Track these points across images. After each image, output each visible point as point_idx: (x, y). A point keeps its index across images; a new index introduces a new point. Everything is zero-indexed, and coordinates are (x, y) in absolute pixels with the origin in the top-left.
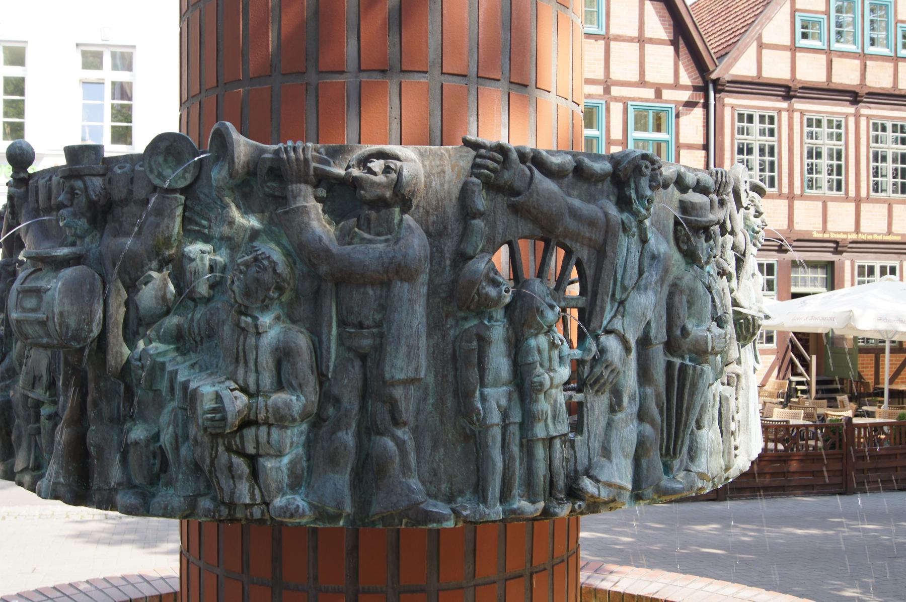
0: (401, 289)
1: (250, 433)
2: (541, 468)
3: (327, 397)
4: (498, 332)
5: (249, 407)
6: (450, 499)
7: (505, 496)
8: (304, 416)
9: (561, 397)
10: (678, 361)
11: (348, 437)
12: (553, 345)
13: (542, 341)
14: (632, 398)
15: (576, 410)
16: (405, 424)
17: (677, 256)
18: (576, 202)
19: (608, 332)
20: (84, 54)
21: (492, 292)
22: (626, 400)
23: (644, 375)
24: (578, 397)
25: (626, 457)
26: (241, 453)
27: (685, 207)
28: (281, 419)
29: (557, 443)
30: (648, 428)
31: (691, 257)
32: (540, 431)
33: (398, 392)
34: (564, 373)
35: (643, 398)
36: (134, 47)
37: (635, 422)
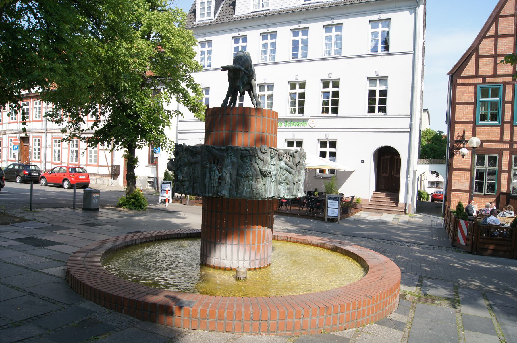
0: (197, 165)
1: (183, 182)
2: (213, 191)
3: (191, 179)
4: (208, 171)
5: (183, 179)
6: (202, 193)
7: (208, 194)
8: (188, 181)
9: (217, 181)
10: (238, 177)
11: (192, 184)
12: (215, 173)
13: (213, 173)
14: (228, 182)
15: (219, 183)
16: (198, 183)
17: (240, 161)
18: (220, 153)
19: (224, 172)
20: (324, 83)
21: (206, 166)
22: (227, 182)
23: (231, 179)
24: (220, 181)
25: (226, 190)
26: (183, 185)
27: (242, 153)
28: (185, 181)
29: (216, 187)
30: (232, 187)
31: (243, 161)
32: (212, 185)
33: (196, 178)
34: (217, 177)
35: (231, 182)
36: (339, 79)
37: (229, 185)
